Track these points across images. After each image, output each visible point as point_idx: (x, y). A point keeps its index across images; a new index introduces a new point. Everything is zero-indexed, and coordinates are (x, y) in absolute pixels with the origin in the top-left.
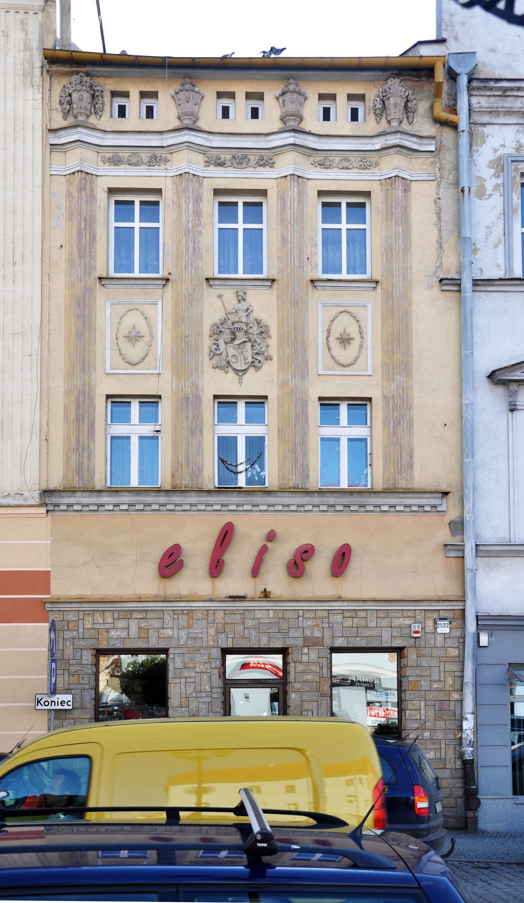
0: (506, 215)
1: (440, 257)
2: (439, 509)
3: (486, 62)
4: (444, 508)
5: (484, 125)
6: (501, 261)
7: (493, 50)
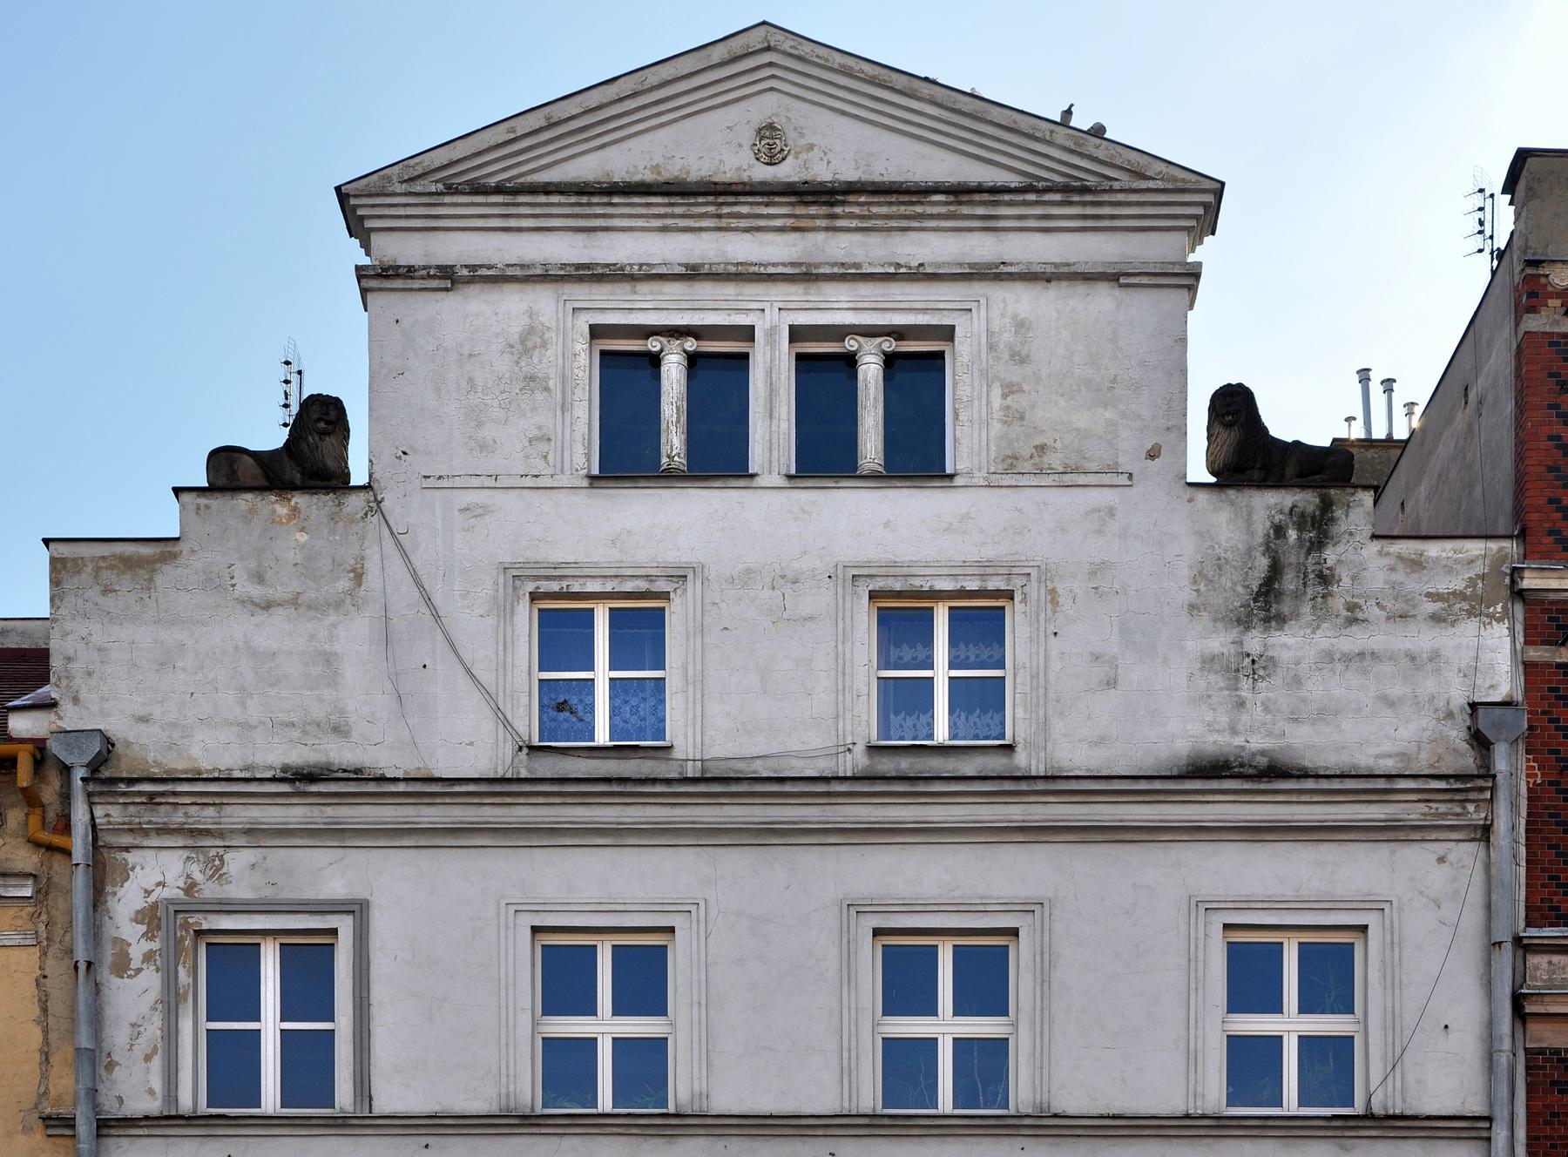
0: (171, 1002)
1: (44, 1076)
3: (131, 739)
5: (127, 849)
6: (157, 1083)
7: (144, 719)
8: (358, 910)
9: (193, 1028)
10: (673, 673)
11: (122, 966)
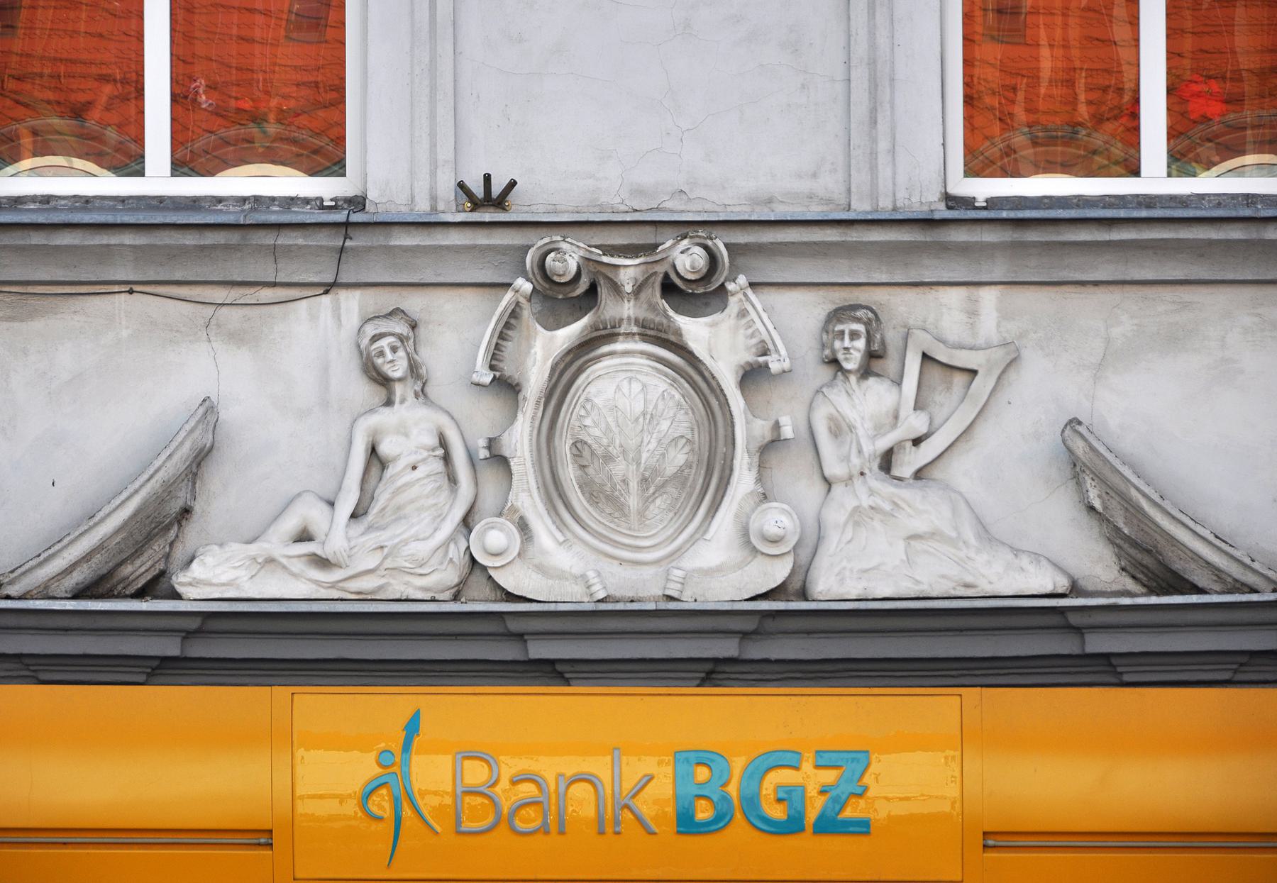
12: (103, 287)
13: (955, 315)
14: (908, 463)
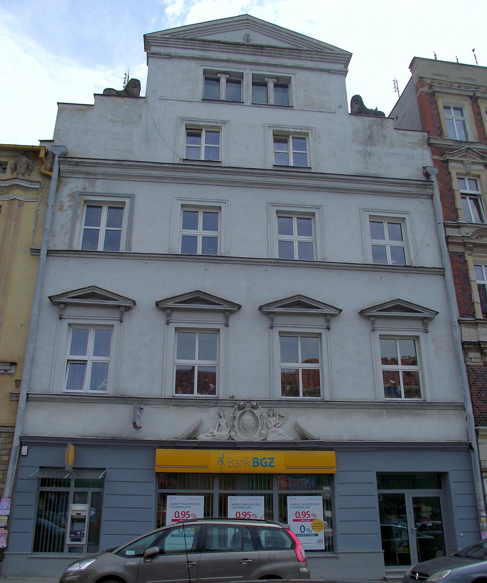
0: (74, 219)
2: (9, 372)
4: (12, 371)
5: (68, 178)
6: (67, 241)
7: (78, 146)
8: (131, 196)
9: (80, 227)
10: (222, 145)
11: (61, 208)
12: (190, 406)
13: (282, 411)
14: (277, 426)
